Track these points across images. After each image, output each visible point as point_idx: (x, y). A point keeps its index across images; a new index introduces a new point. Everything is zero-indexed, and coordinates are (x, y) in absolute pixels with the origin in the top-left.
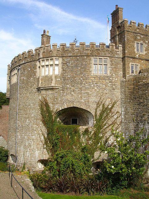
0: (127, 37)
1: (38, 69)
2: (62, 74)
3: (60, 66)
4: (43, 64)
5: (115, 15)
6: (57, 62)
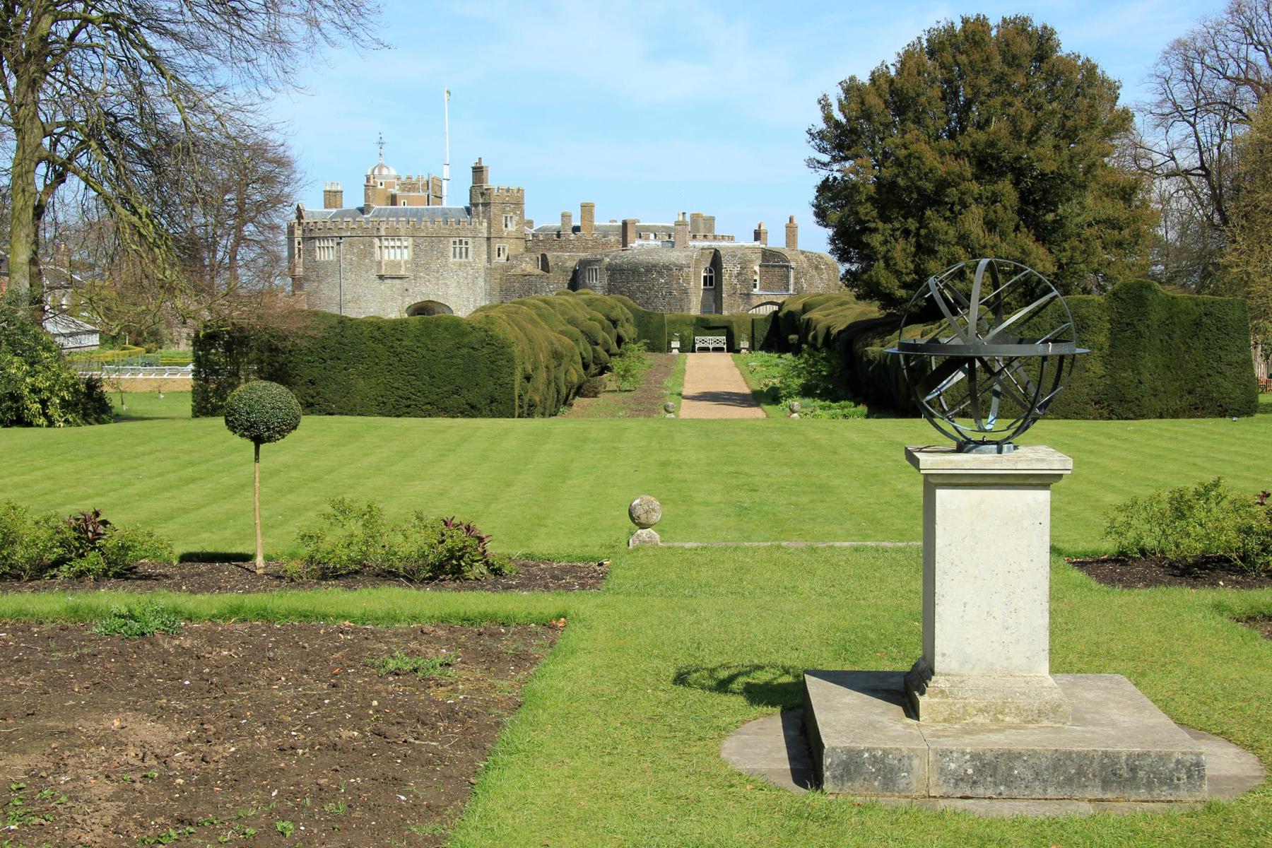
0: (494, 210)
1: (377, 250)
2: (414, 259)
3: (411, 248)
4: (386, 243)
5: (478, 171)
6: (405, 244)
